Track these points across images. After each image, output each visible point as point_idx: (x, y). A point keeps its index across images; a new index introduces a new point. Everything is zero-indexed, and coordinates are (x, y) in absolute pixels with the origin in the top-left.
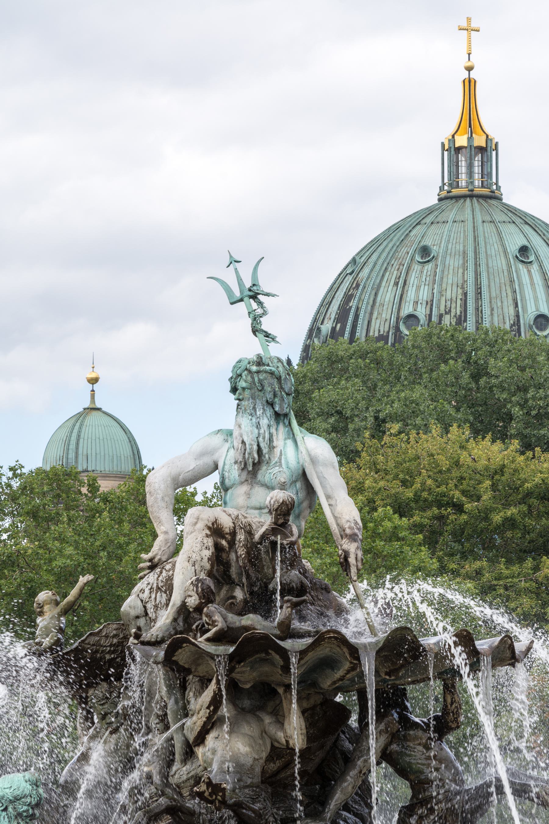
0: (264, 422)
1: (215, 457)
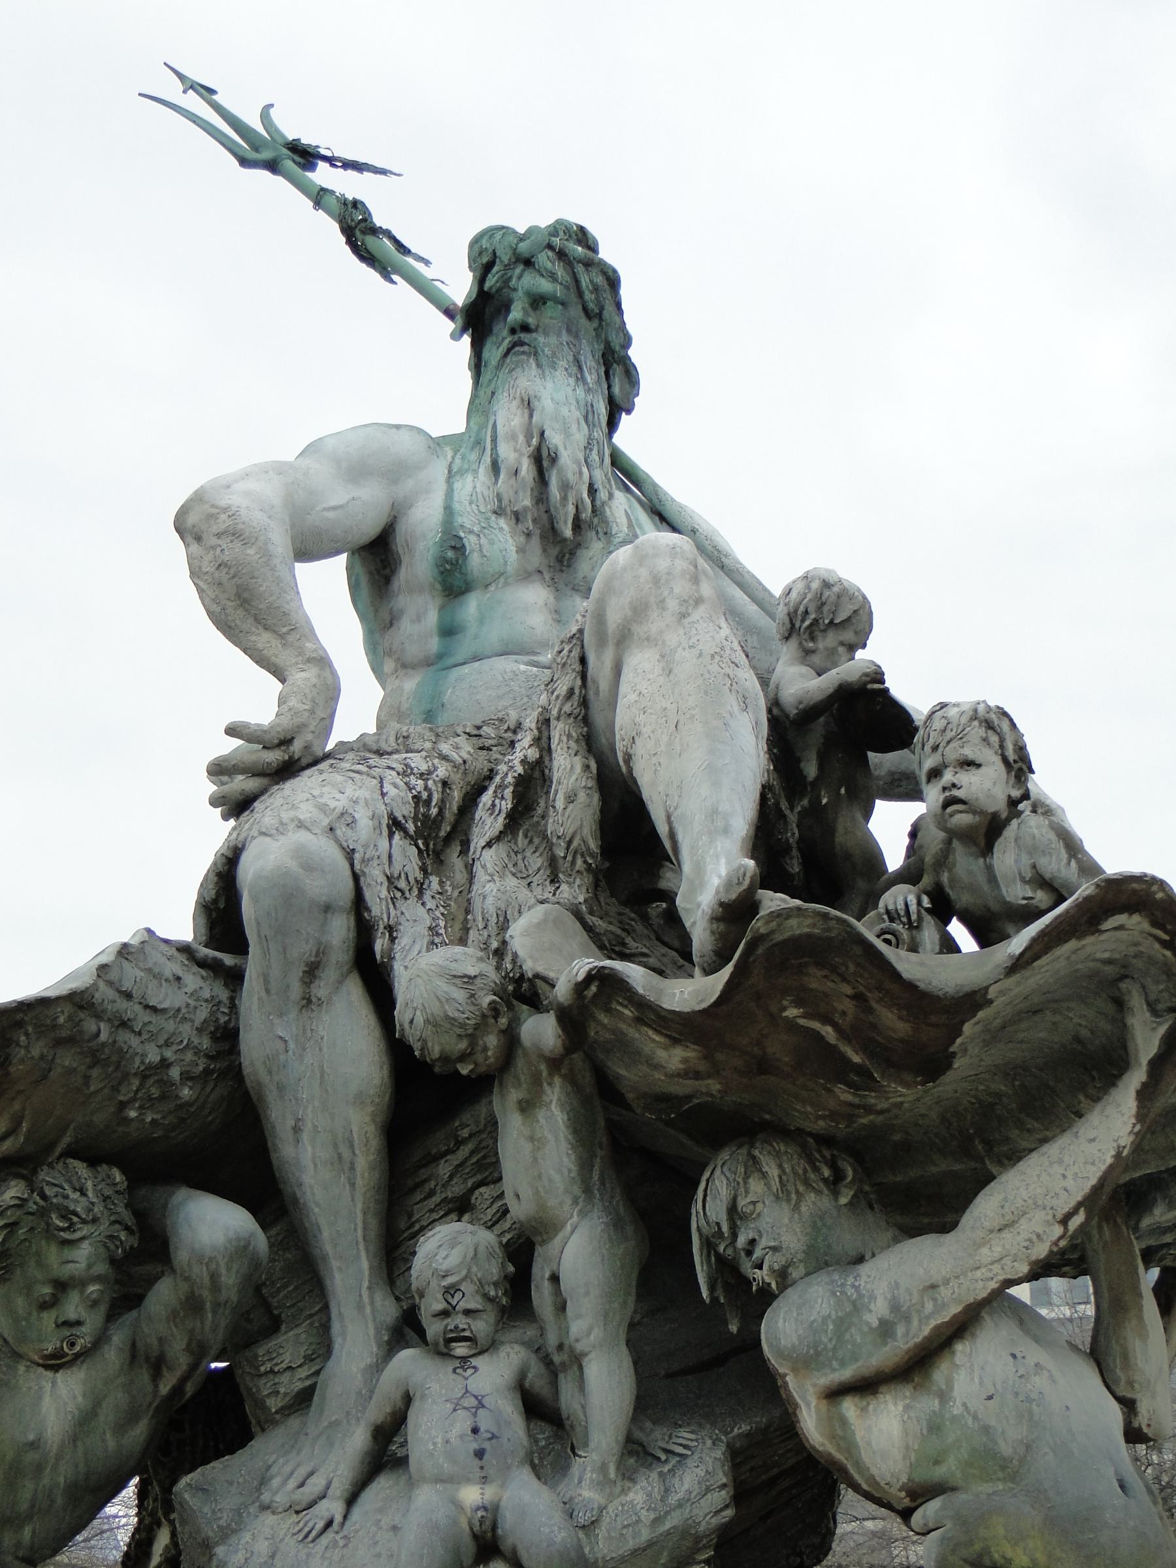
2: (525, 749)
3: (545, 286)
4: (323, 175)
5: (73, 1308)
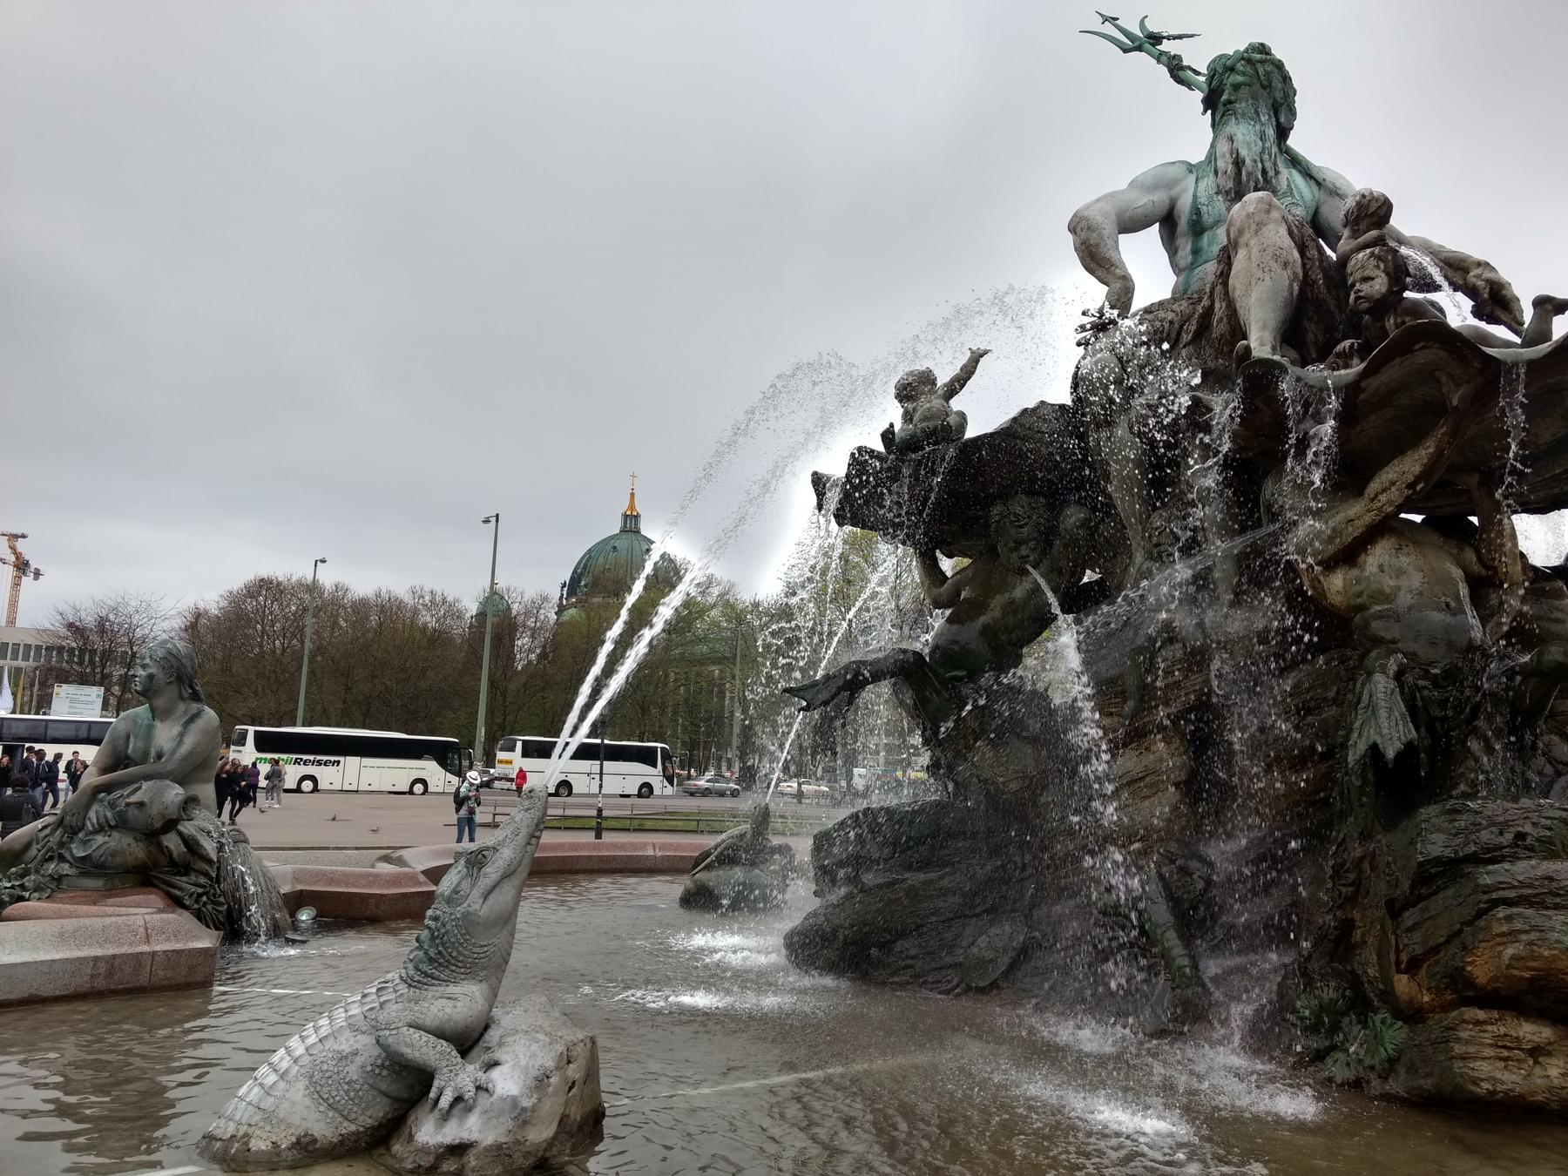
0: (1271, 132)
1: (1174, 192)
2: (1205, 302)
3: (1240, 79)
4: (1166, 46)
5: (1024, 551)
